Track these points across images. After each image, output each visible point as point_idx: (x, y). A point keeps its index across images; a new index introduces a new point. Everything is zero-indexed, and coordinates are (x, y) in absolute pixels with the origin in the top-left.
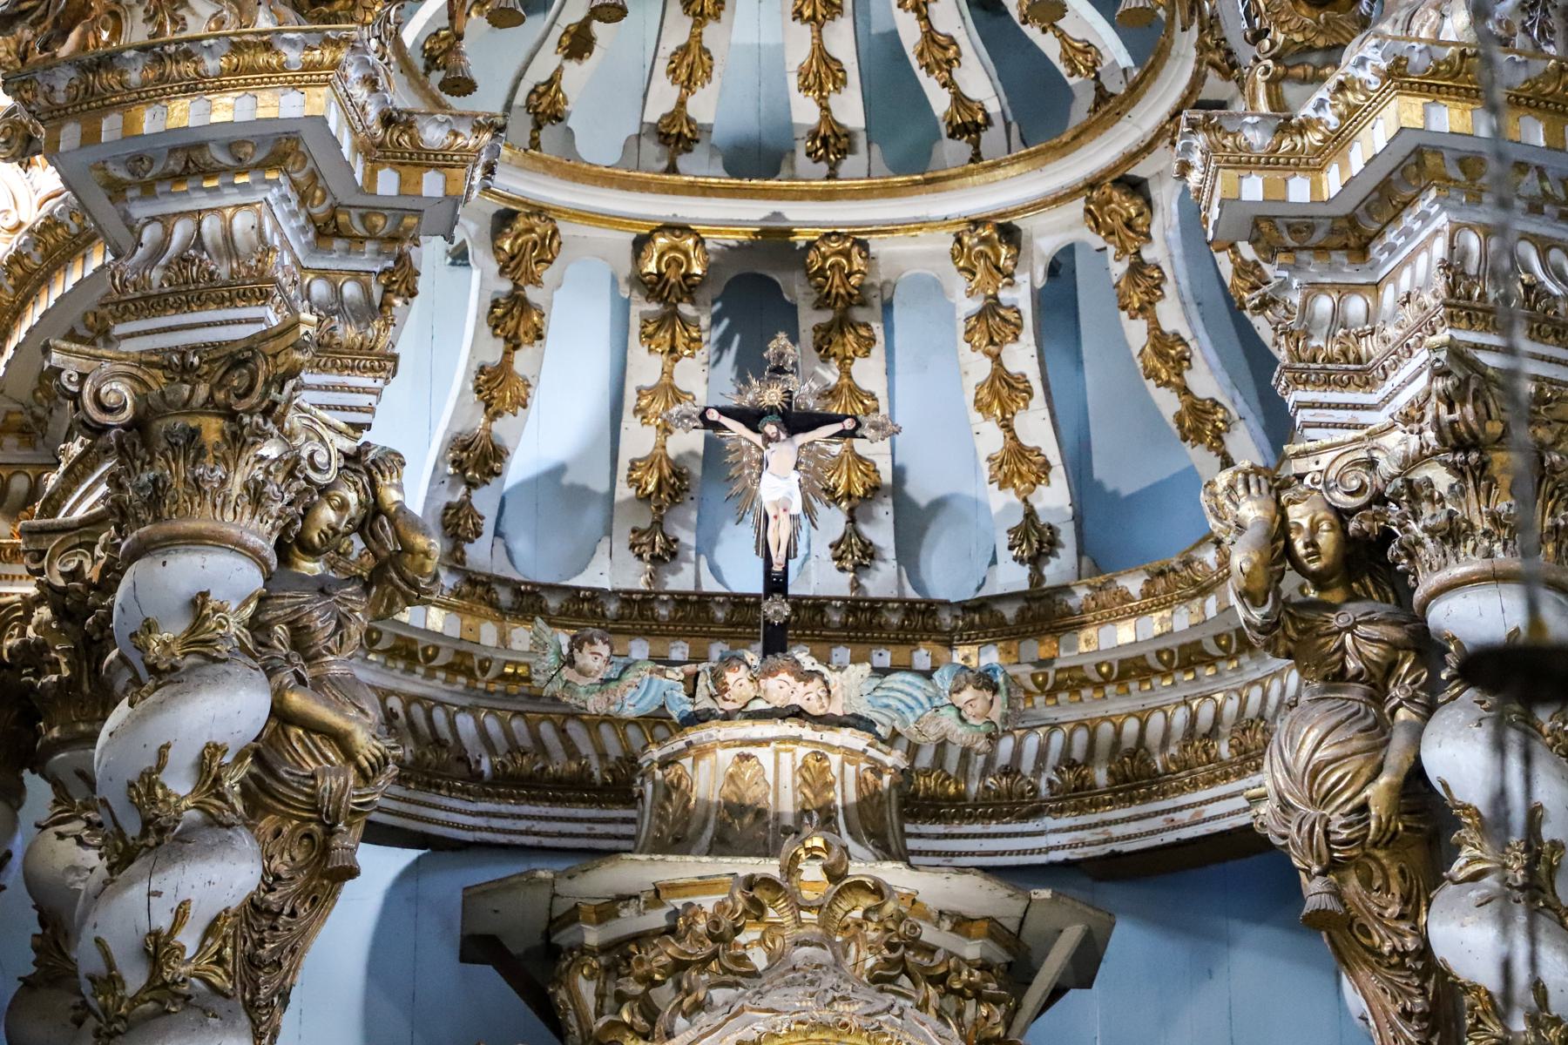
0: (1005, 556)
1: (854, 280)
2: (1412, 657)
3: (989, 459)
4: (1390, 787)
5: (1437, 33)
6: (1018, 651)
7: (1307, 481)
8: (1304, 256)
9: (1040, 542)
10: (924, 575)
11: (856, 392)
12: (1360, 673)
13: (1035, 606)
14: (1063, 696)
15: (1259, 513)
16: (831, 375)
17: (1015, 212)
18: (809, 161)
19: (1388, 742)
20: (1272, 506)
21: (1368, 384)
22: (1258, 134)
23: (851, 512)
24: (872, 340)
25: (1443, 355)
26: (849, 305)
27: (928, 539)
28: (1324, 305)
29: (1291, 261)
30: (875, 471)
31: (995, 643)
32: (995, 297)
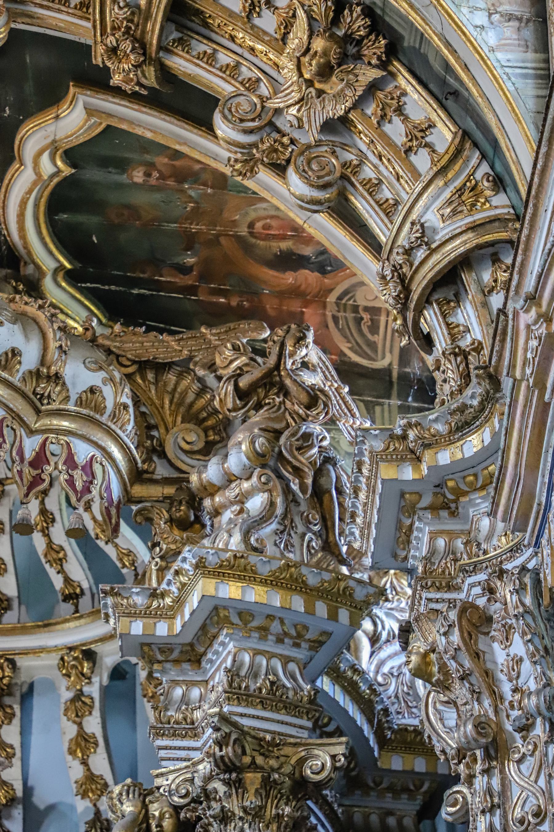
5: (227, 544)
8: (168, 665)
21: (196, 736)
22: (140, 598)
25: (216, 719)
28: (178, 692)
29: (161, 668)
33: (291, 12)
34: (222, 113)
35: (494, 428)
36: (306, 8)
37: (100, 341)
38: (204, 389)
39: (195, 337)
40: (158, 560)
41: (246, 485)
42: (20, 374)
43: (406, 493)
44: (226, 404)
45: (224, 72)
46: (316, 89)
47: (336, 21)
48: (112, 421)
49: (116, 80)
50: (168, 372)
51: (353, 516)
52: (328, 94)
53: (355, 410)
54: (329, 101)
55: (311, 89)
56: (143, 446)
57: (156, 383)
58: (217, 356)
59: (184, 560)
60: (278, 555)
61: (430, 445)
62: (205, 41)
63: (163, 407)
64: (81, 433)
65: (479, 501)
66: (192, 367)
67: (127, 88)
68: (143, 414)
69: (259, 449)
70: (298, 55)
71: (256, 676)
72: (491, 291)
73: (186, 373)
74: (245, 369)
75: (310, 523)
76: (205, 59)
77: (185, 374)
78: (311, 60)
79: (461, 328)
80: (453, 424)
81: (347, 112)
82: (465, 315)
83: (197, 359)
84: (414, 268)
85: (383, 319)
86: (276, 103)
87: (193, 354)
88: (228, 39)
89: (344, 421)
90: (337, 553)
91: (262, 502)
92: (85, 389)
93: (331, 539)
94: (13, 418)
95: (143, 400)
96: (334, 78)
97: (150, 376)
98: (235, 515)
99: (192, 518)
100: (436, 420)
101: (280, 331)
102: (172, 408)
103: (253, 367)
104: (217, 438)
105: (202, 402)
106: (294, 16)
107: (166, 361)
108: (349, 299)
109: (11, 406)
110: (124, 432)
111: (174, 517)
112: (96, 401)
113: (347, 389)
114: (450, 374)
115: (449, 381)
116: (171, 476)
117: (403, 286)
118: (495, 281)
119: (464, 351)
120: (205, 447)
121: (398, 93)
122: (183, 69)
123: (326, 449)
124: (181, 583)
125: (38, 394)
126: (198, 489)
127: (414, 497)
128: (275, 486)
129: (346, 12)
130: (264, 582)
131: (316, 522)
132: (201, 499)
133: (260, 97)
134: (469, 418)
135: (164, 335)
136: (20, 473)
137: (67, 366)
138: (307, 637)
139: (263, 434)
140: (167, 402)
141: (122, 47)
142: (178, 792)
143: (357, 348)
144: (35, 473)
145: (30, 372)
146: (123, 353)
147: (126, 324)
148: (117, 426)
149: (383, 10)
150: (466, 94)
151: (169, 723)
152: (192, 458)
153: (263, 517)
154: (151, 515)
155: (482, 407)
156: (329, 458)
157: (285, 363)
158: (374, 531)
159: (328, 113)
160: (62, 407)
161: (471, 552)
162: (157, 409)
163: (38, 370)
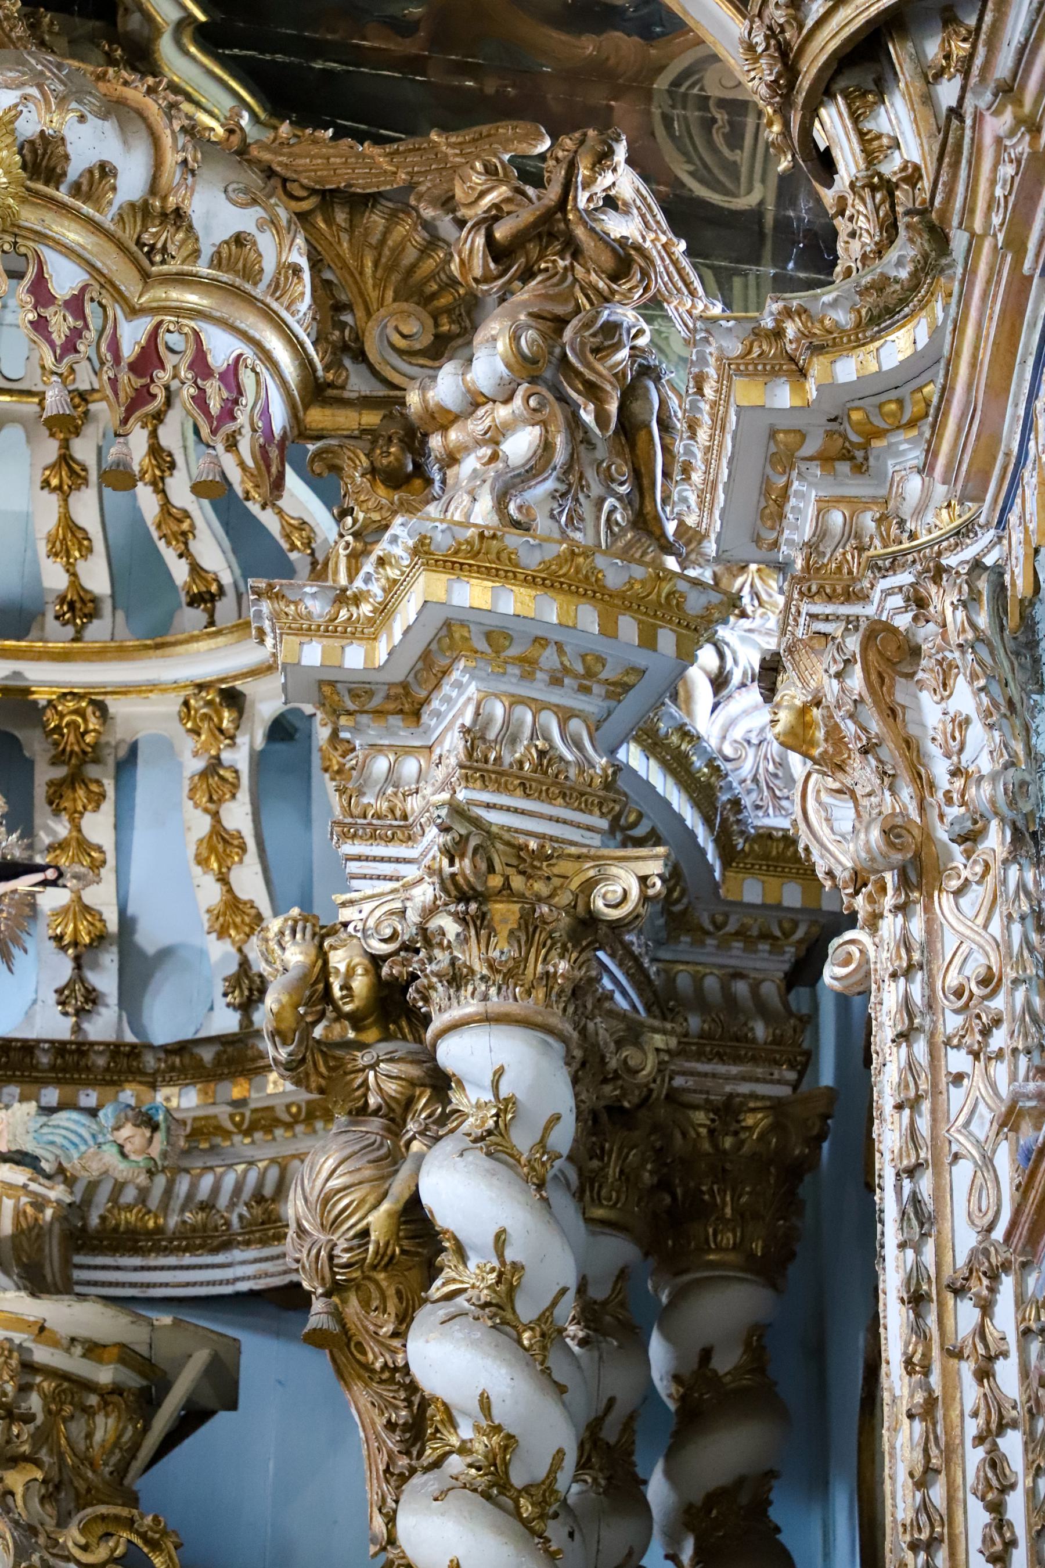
0: (220, 1002)
1: (89, 739)
2: (428, 1093)
3: (208, 911)
4: (390, 1214)
5: (468, 515)
6: (215, 1092)
7: (350, 928)
8: (364, 719)
9: (251, 990)
10: (145, 1020)
11: (84, 846)
12: (379, 1108)
13: (230, 1049)
14: (258, 1135)
15: (301, 958)
16: (62, 829)
17: (236, 678)
18: (57, 624)
19: (397, 1171)
20: (313, 952)
23: (77, 959)
24: (103, 796)
26: (83, 762)
27: (152, 988)
29: (352, 724)
30: (101, 920)
31: (194, 1084)
32: (218, 758)
35: (936, 319)
37: (255, 152)
38: (434, 241)
39: (419, 149)
40: (350, 538)
41: (503, 412)
42: (114, 209)
43: (778, 431)
44: (470, 269)
48: (272, 295)
50: (372, 212)
51: (687, 469)
53: (697, 284)
56: (326, 340)
57: (351, 230)
58: (457, 183)
59: (394, 539)
60: (557, 535)
61: (822, 347)
63: (361, 273)
64: (218, 314)
65: (904, 446)
66: (413, 202)
68: (328, 283)
69: (526, 350)
71: (514, 740)
72: (939, 75)
73: (403, 212)
74: (506, 208)
75: (613, 480)
77: (401, 215)
79: (885, 141)
80: (864, 312)
82: (893, 117)
83: (423, 188)
84: (805, 31)
85: (751, 121)
87: (415, 179)
89: (675, 303)
90: (658, 532)
91: (530, 444)
92: (226, 237)
93: (648, 508)
94: (102, 286)
95: (328, 259)
97: (341, 217)
98: (484, 464)
99: (410, 467)
100: (834, 304)
101: (568, 141)
102: (379, 274)
103: (518, 205)
104: (455, 328)
105: (429, 265)
107: (368, 191)
108: (692, 86)
109: (99, 265)
110: (293, 315)
111: (377, 465)
112: (245, 260)
113: (683, 245)
114: (862, 222)
115: (861, 235)
116: (375, 394)
117: (785, 64)
118: (947, 57)
119: (889, 181)
120: (433, 343)
123: (644, 352)
124: (388, 579)
125: (145, 245)
126: (421, 418)
127: (791, 438)
128: (552, 414)
130: (531, 581)
131: (623, 479)
132: (426, 435)
134: (892, 301)
135: (366, 144)
136: (114, 382)
137: (196, 196)
138: (603, 676)
139: (534, 324)
140: (369, 264)
142: (378, 933)
143: (705, 172)
144: (138, 382)
145: (132, 205)
146: (295, 176)
147: (299, 124)
148: (282, 304)
151: (365, 817)
152: (410, 363)
153: (532, 468)
154: (338, 462)
155: (915, 282)
156: (649, 367)
157: (575, 198)
158: (722, 497)
160: (186, 268)
161: (888, 535)
162: (352, 275)
163: (146, 202)
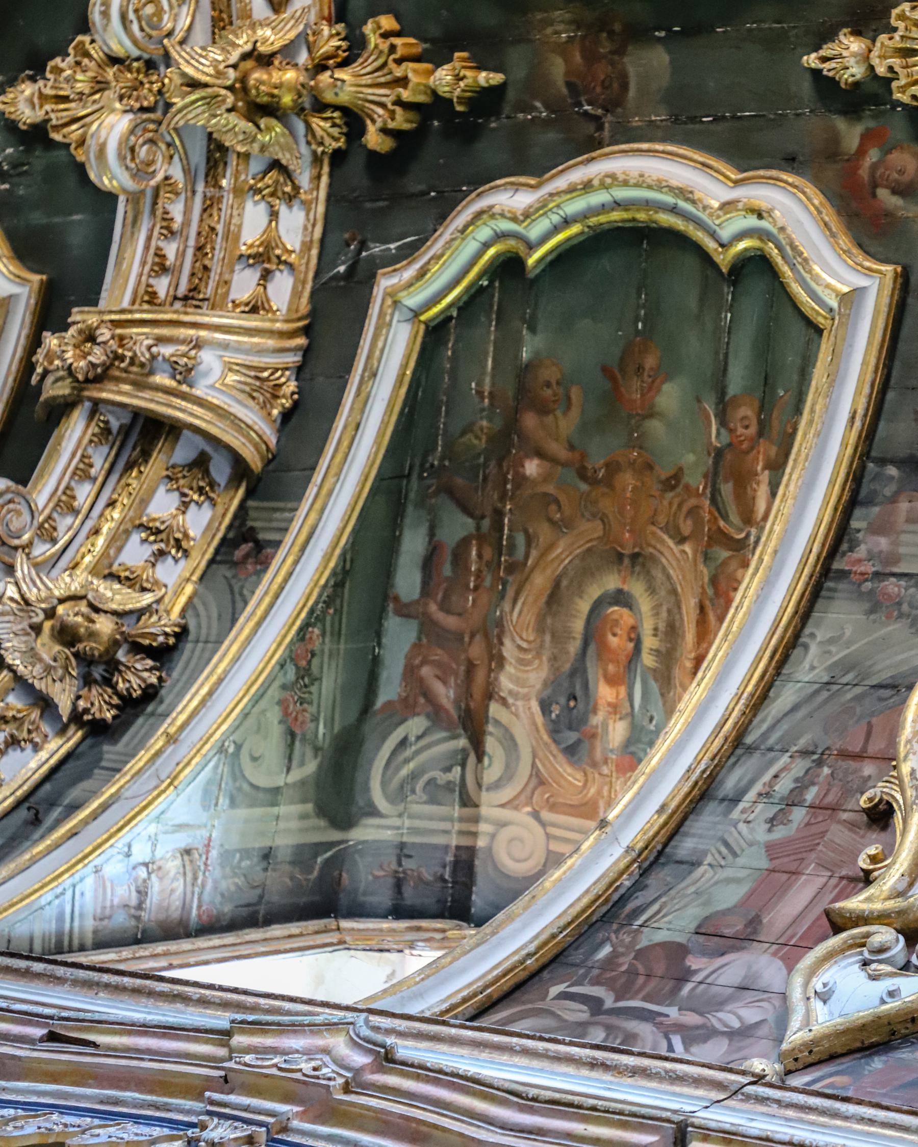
33: (149, 586)
34: (8, 490)
36: (154, 606)
45: (64, 493)
46: (41, 624)
47: (137, 648)
49: (51, 341)
52: (35, 641)
54: (25, 642)
55: (42, 616)
62: (107, 465)
67: (40, 356)
70: (90, 597)
76: (81, 466)
78: (83, 615)
81: (10, 668)
86: (22, 568)
88: (110, 498)
96: (57, 648)
106: (144, 590)
121: (37, 740)
122: (67, 434)
129: (150, 663)
133: (30, 544)
141: (97, 350)
149: (152, 714)
150: (36, 836)
159: (9, 641)
